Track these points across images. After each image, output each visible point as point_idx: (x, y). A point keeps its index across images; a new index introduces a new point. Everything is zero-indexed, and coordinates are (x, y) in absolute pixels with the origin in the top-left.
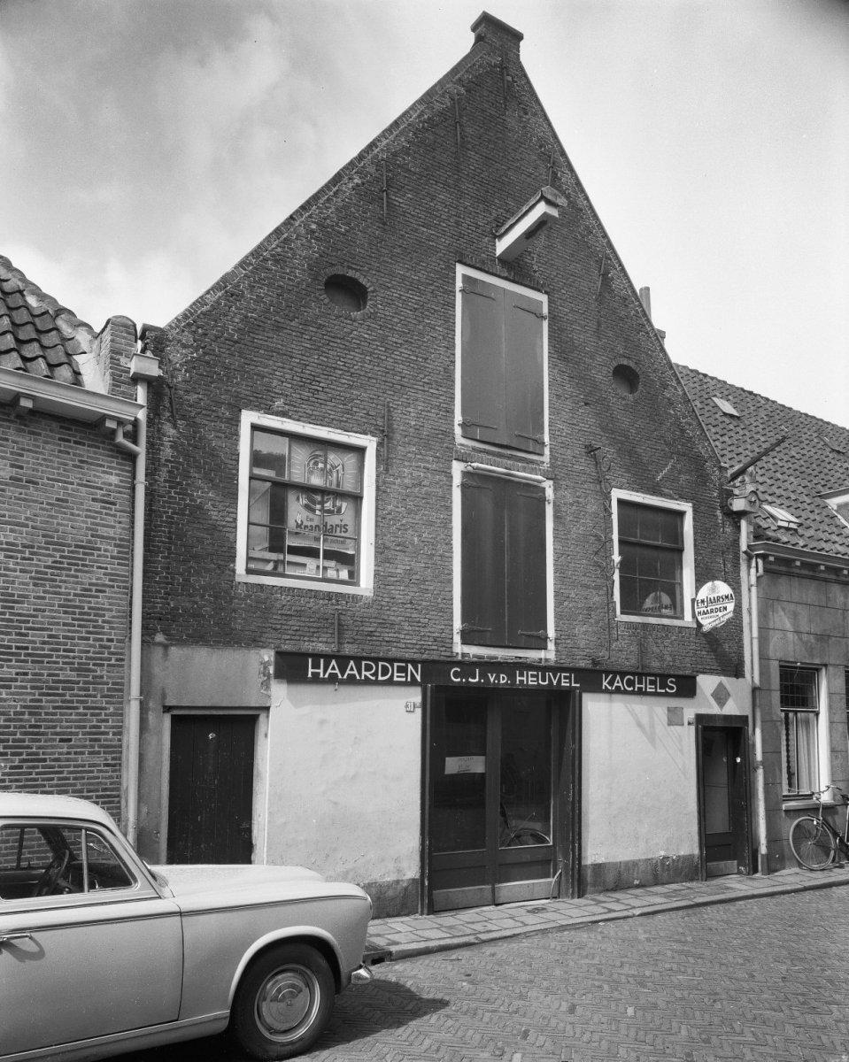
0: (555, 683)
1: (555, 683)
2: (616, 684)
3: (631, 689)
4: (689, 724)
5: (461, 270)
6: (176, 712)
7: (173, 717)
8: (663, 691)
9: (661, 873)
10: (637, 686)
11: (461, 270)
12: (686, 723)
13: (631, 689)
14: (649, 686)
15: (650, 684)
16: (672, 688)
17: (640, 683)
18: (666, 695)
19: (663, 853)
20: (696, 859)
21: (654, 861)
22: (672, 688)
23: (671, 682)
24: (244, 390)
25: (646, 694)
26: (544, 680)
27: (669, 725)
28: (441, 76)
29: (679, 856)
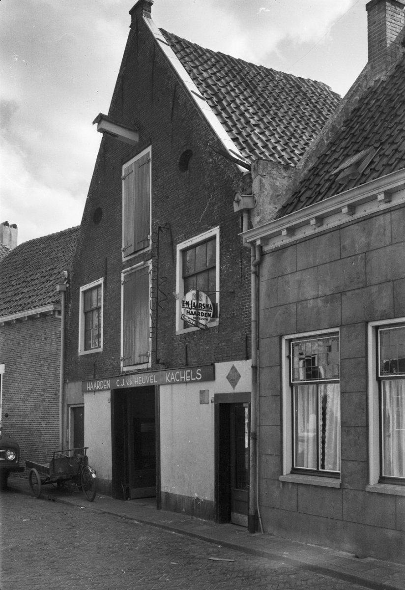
0: (148, 382)
1: (148, 382)
2: (172, 378)
3: (178, 380)
4: (212, 402)
5: (216, 231)
6: (72, 406)
7: (72, 408)
8: (194, 379)
9: (194, 507)
10: (181, 378)
11: (216, 231)
12: (210, 401)
13: (178, 380)
14: (187, 377)
15: (188, 376)
16: (199, 376)
17: (183, 376)
18: (197, 381)
19: (196, 495)
20: (110, 482)
21: (192, 500)
22: (199, 376)
23: (199, 372)
24: (78, 286)
25: (186, 382)
26: (144, 381)
27: (201, 403)
28: (118, 72)
29: (205, 500)
